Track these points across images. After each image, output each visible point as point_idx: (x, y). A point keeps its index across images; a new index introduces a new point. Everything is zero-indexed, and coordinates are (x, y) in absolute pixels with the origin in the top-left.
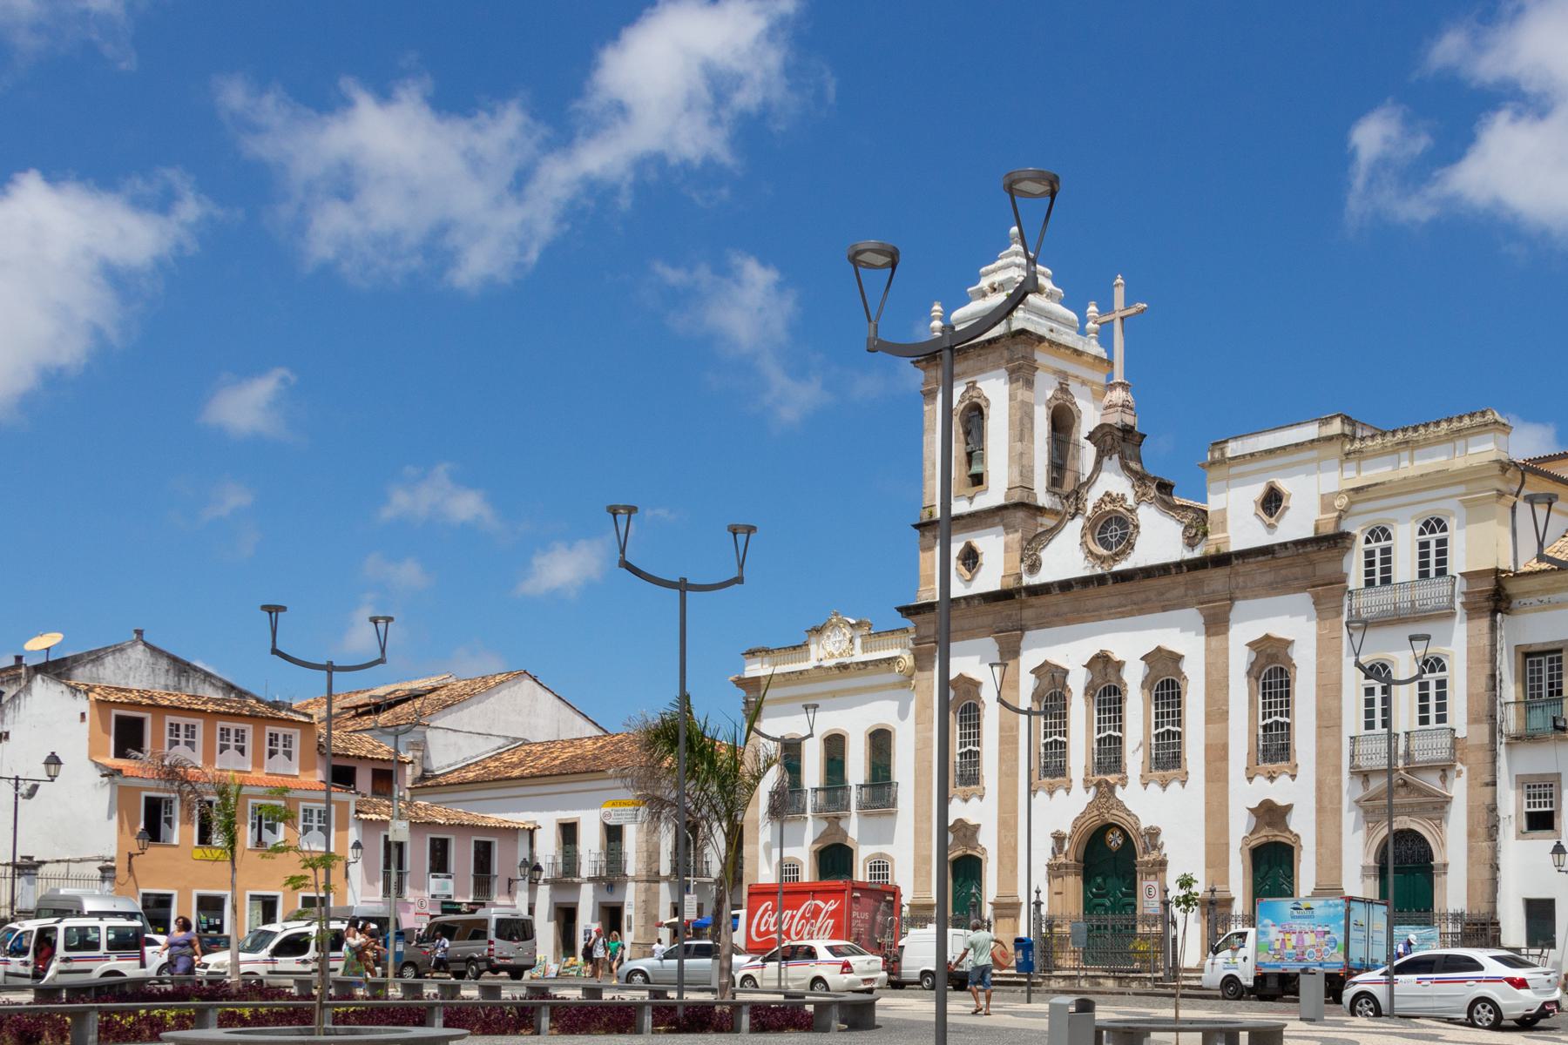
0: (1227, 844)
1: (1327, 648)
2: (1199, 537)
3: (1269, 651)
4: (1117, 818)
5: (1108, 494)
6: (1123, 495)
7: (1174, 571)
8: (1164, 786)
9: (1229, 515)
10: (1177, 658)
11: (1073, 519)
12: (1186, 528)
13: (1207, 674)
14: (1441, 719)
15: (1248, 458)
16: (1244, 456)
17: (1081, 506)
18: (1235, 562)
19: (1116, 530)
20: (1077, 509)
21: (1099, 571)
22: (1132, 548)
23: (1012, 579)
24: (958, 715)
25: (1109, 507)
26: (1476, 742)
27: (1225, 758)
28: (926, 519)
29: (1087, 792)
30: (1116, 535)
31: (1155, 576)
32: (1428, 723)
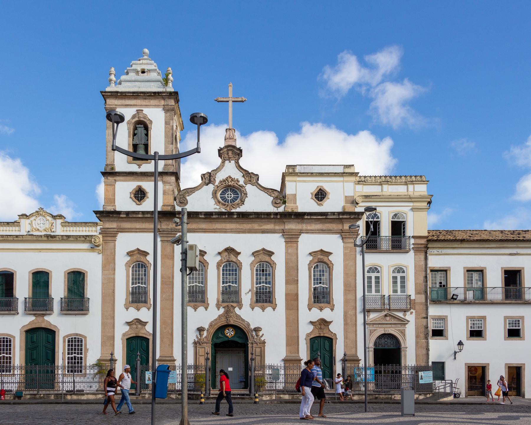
0: (298, 337)
1: (350, 260)
3: (319, 256)
4: (237, 323)
5: (230, 177)
8: (263, 309)
10: (270, 253)
11: (207, 185)
13: (286, 263)
14: (403, 291)
16: (308, 173)
17: (212, 180)
21: (224, 210)
24: (131, 269)
26: (419, 301)
27: (297, 299)
28: (108, 170)
29: (218, 310)
32: (397, 293)
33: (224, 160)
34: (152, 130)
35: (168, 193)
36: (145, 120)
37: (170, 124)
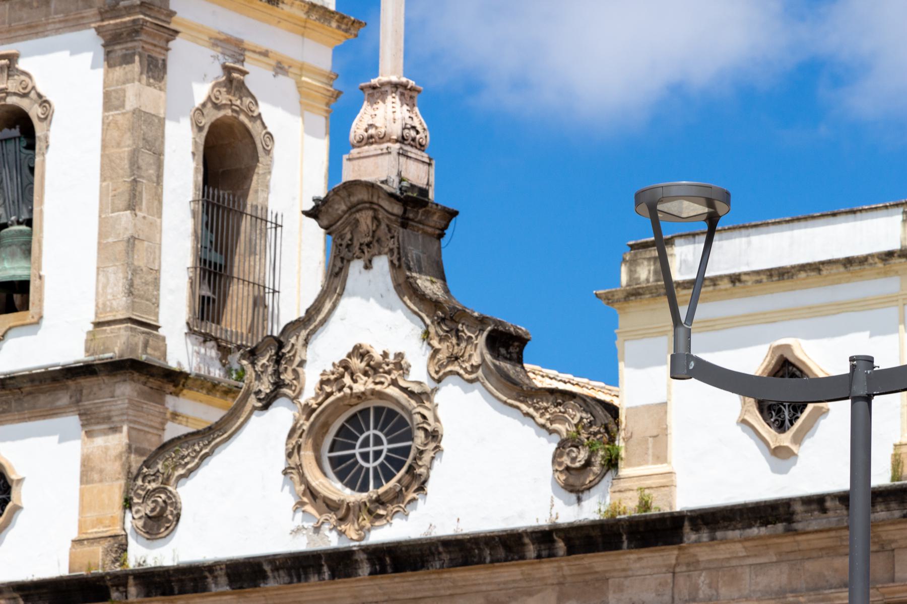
2: (596, 469)
5: (360, 352)
6: (400, 356)
7: (531, 550)
9: (673, 420)
11: (266, 407)
12: (562, 445)
15: (725, 285)
18: (690, 536)
19: (378, 441)
20: (278, 385)
21: (331, 540)
22: (421, 488)
23: (99, 550)
25: (362, 385)
30: (377, 454)
31: (481, 561)
33: (339, 264)
34: (48, 156)
35: (101, 471)
36: (24, 104)
37: (123, 106)
